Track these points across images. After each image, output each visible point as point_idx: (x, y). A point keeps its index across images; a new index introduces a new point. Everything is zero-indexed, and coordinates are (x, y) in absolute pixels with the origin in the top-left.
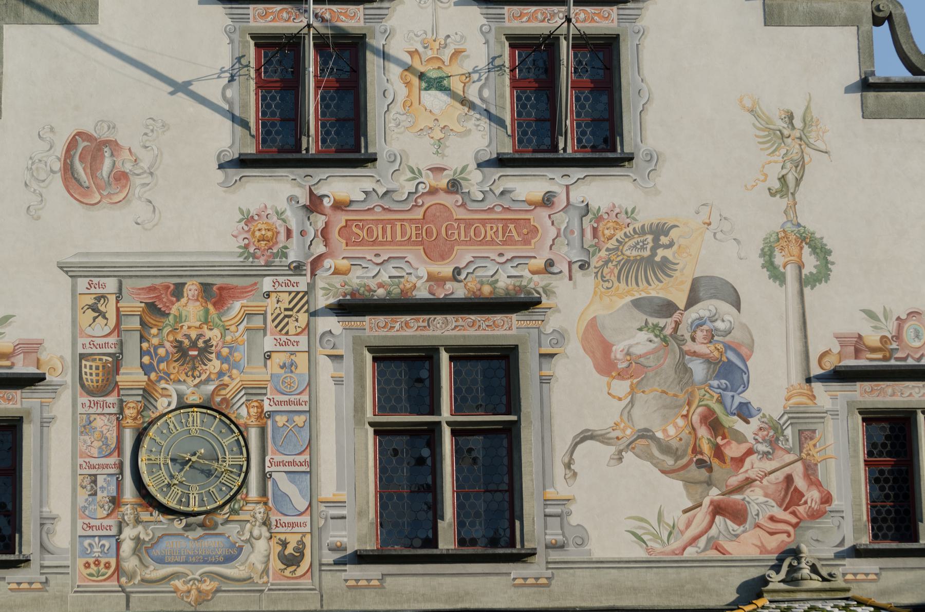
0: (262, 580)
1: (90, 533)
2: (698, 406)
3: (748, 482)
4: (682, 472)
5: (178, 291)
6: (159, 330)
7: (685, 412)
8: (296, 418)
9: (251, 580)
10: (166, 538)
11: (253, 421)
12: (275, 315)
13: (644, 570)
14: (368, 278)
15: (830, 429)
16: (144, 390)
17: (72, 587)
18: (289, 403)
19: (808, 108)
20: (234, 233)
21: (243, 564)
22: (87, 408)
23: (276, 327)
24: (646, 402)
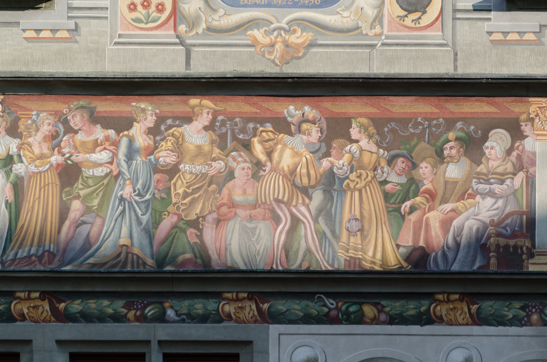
0: (373, 31)
9: (359, 31)
17: (111, 36)
21: (347, 8)
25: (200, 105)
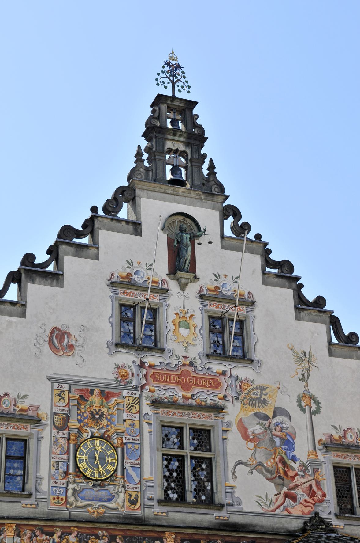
1: (55, 485)
2: (278, 455)
3: (296, 486)
4: (274, 480)
5: (92, 392)
6: (84, 406)
7: (273, 457)
8: (135, 446)
10: (85, 490)
11: (119, 445)
12: (127, 405)
13: (262, 517)
14: (161, 394)
15: (324, 468)
16: (78, 429)
18: (132, 439)
19: (310, 350)
20: (113, 372)
22: (56, 435)
23: (128, 409)
24: (260, 452)
25: (74, 529)
